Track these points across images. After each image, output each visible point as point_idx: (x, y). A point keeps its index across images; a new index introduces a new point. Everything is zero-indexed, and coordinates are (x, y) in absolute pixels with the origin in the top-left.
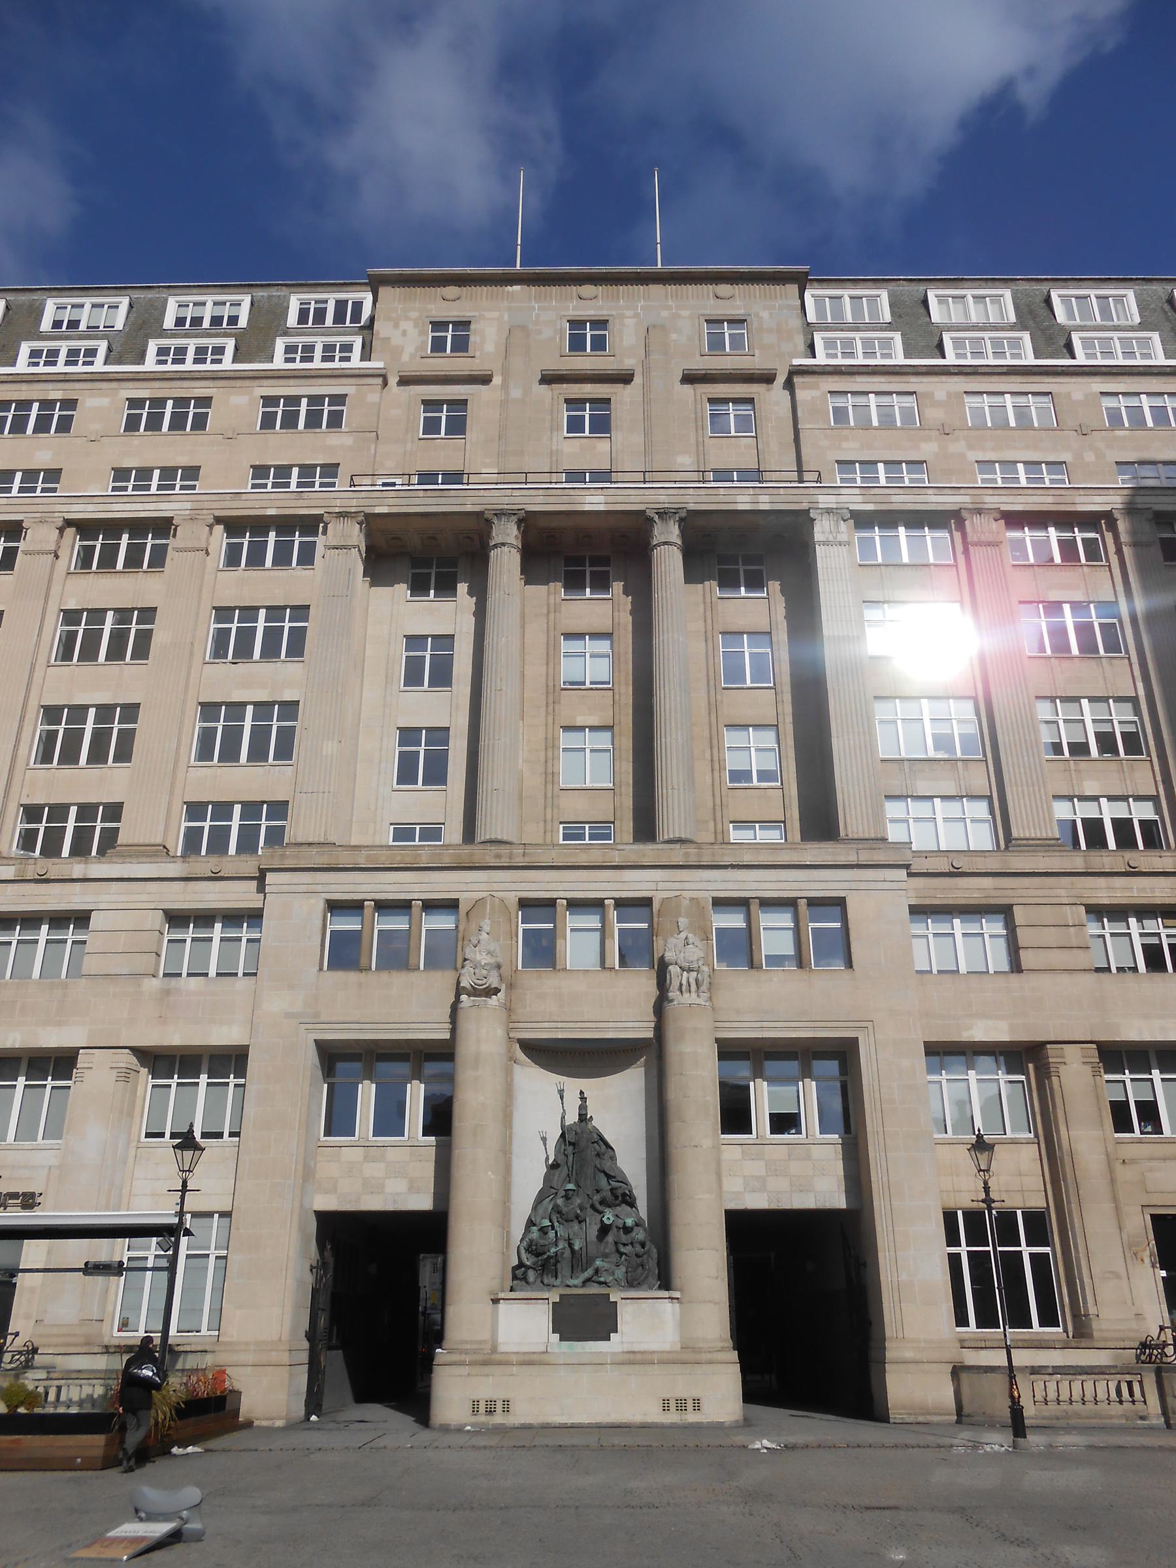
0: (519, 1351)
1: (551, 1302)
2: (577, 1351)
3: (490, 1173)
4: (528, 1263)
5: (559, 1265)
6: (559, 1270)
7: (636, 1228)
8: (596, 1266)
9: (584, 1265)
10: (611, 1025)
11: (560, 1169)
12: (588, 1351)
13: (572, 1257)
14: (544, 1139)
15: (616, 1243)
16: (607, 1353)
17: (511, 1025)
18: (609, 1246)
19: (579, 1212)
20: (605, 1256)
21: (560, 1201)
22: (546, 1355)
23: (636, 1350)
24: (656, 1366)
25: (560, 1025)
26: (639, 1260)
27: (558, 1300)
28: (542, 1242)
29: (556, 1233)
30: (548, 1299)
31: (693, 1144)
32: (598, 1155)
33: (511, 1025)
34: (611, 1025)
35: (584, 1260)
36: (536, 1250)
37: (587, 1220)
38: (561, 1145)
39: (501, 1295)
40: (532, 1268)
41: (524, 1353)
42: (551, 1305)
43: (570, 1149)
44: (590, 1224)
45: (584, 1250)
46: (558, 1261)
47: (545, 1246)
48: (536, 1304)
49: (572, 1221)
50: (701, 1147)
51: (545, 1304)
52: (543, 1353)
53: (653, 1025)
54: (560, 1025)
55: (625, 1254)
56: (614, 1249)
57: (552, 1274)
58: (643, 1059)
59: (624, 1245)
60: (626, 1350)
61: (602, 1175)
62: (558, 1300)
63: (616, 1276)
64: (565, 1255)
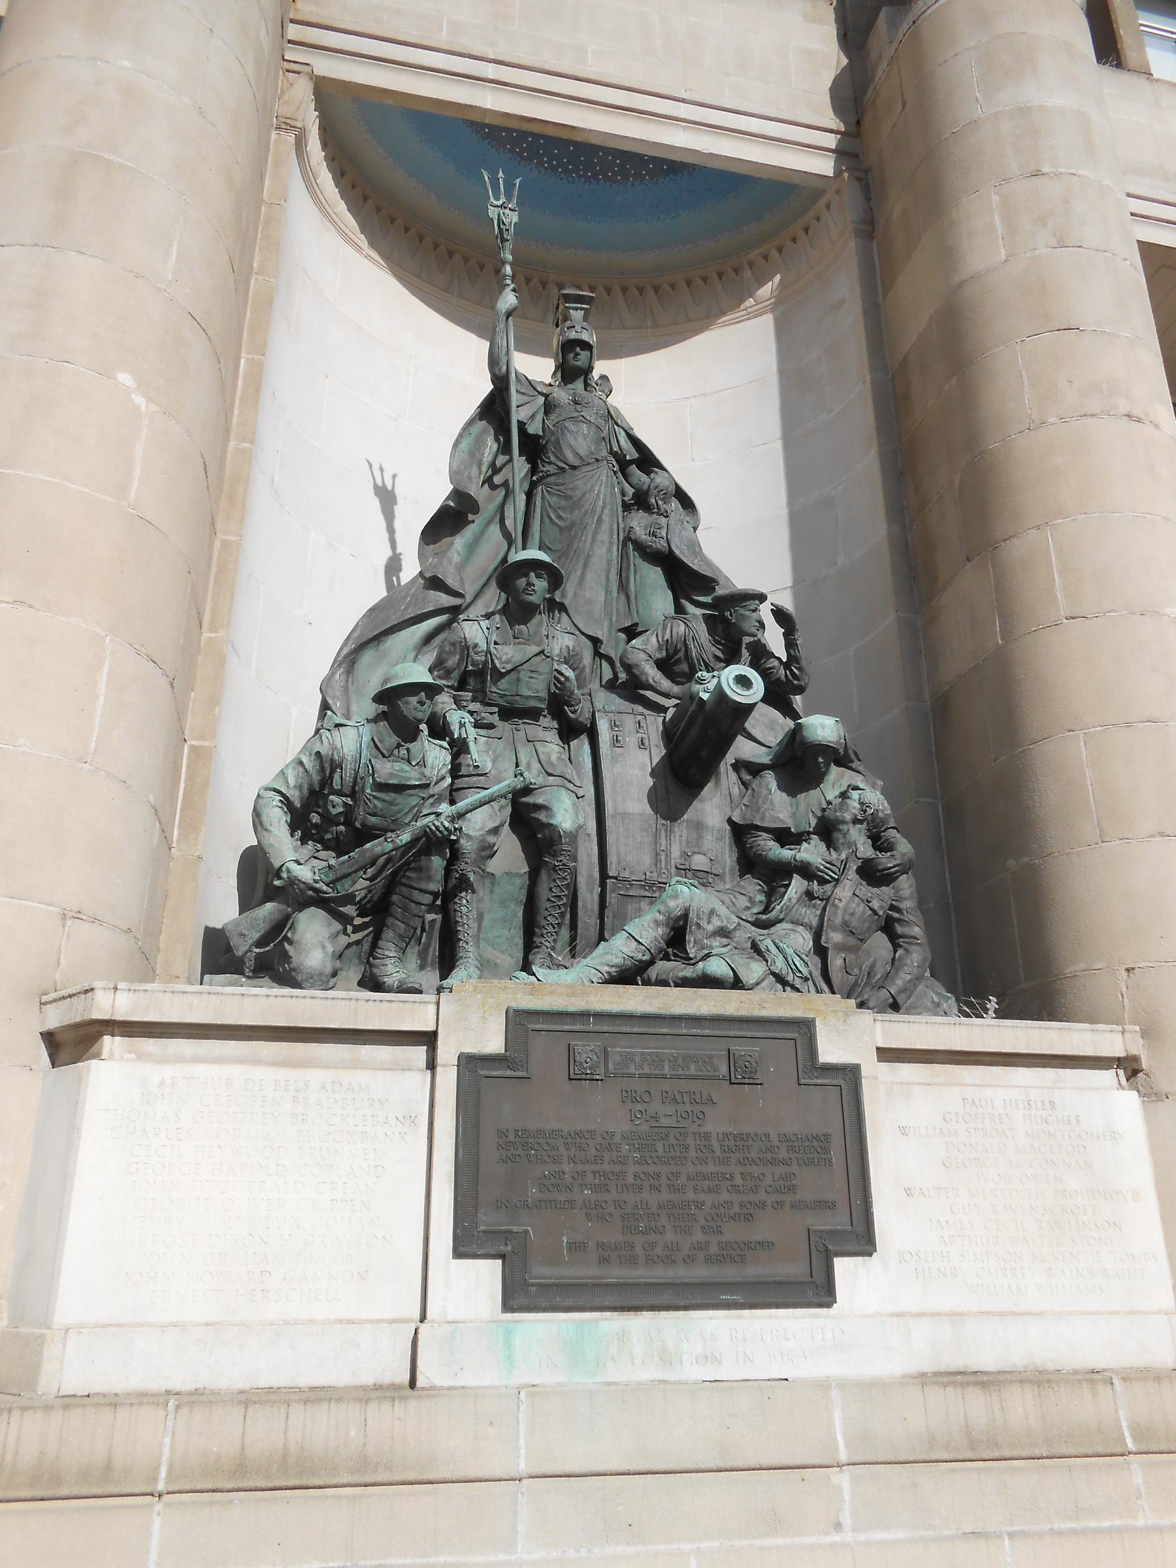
0: (205, 1380)
1: (447, 1053)
2: (615, 1374)
3: (125, 378)
4: (305, 873)
5: (466, 905)
6: (467, 928)
7: (835, 771)
8: (675, 906)
9: (588, 919)
10: (683, 111)
11: (469, 532)
12: (694, 1372)
13: (534, 875)
14: (387, 498)
15: (740, 833)
16: (823, 1386)
17: (293, 31)
18: (709, 841)
19: (569, 673)
20: (703, 878)
21: (474, 631)
22: (411, 1409)
23: (987, 1361)
24: (1136, 1471)
25: (491, 71)
26: (880, 898)
27: (493, 1042)
28: (387, 770)
29: (459, 748)
30: (428, 1039)
31: (1123, 408)
32: (641, 501)
33: (293, 31)
34: (683, 111)
35: (588, 897)
36: (349, 812)
37: (603, 726)
38: (479, 444)
39: (105, 1005)
40: (321, 902)
41: (247, 1399)
42: (448, 1077)
43: (521, 466)
44: (616, 742)
45: (588, 851)
46: (464, 884)
47: (400, 788)
48: (357, 1065)
49: (533, 714)
50: (1157, 426)
51: (396, 1067)
52: (382, 1392)
53: (831, 141)
54: (491, 71)
55: (806, 871)
56: (728, 857)
57: (423, 955)
58: (766, 290)
59: (784, 837)
60: (928, 1367)
61: (654, 576)
62: (493, 1042)
63: (780, 965)
64: (493, 866)
